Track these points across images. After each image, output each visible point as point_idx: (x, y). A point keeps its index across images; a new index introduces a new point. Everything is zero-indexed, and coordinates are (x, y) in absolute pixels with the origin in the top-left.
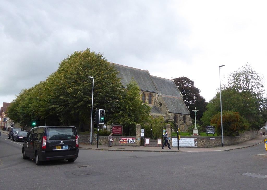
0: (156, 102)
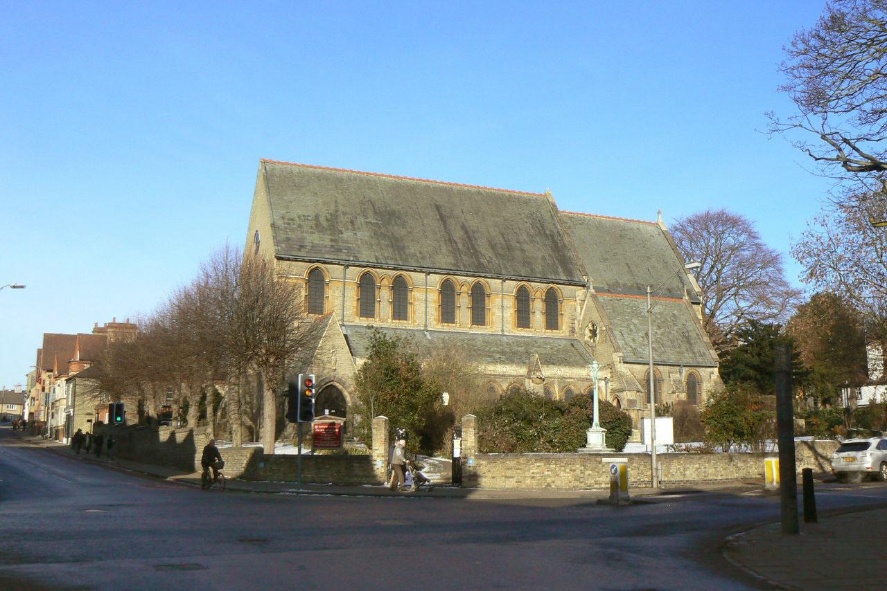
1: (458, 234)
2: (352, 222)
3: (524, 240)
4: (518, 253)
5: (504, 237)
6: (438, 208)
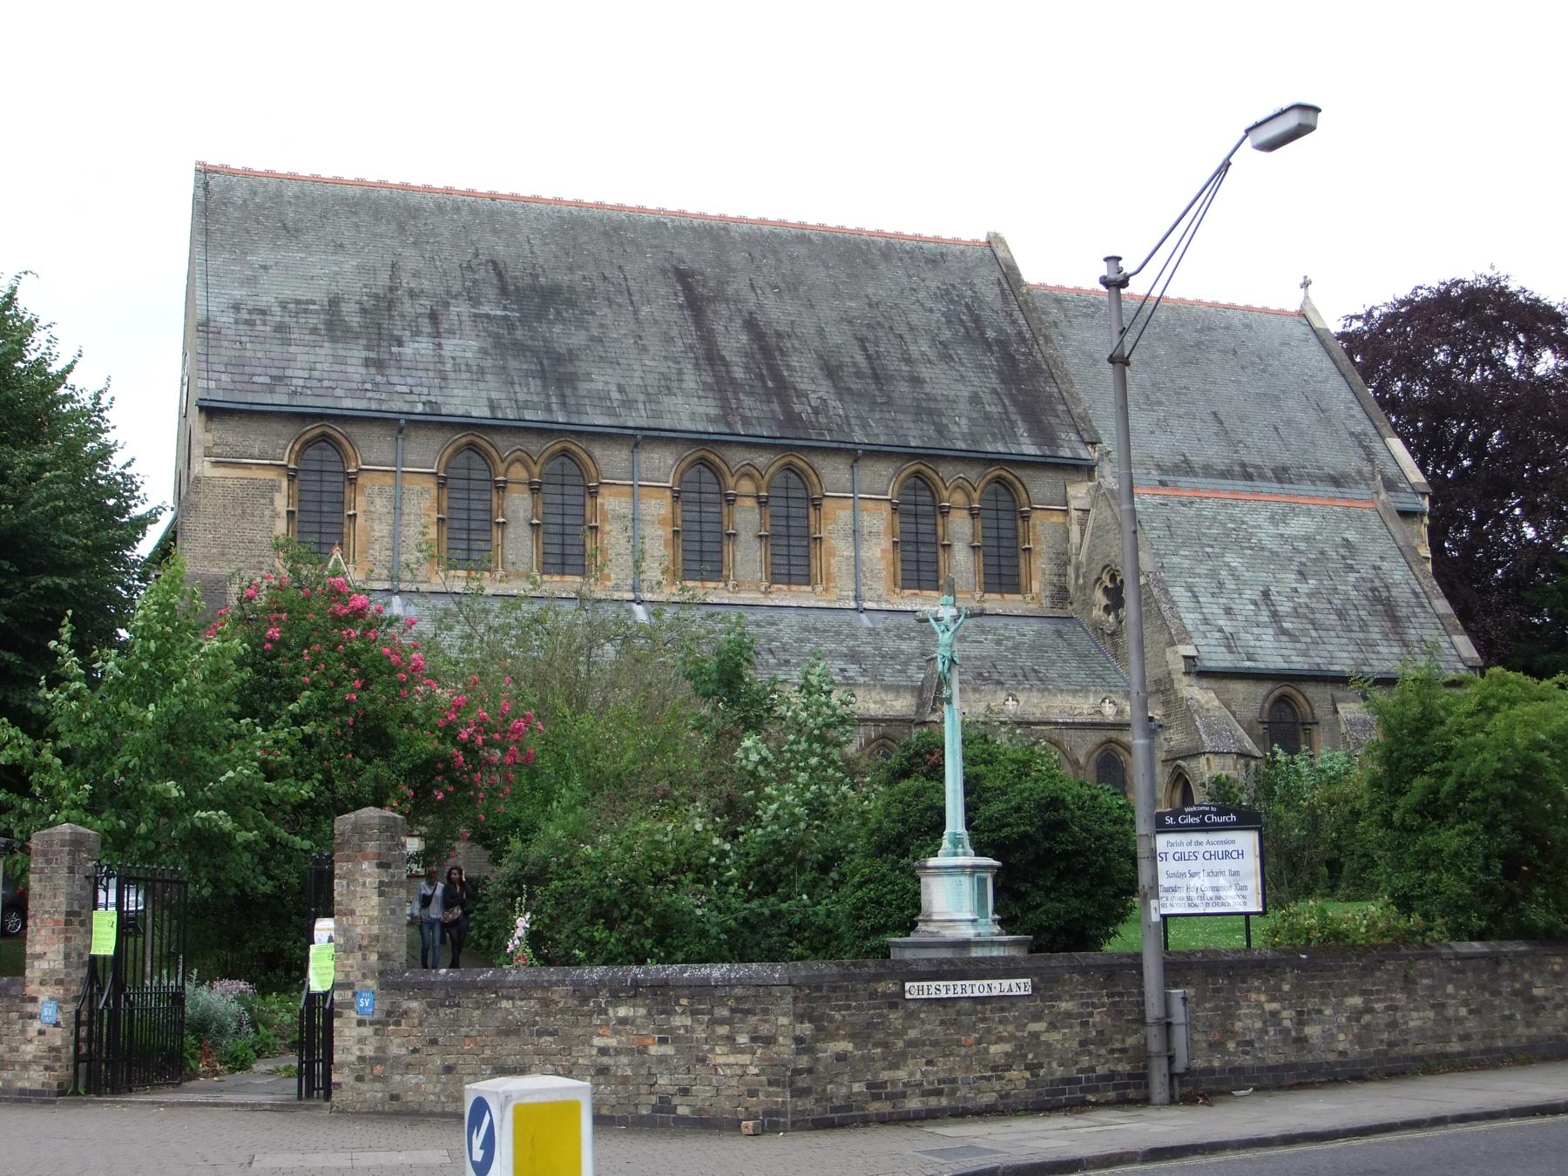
0: (1071, 570)
1: (733, 343)
2: (434, 317)
3: (923, 354)
4: (904, 387)
5: (865, 349)
6: (683, 276)
